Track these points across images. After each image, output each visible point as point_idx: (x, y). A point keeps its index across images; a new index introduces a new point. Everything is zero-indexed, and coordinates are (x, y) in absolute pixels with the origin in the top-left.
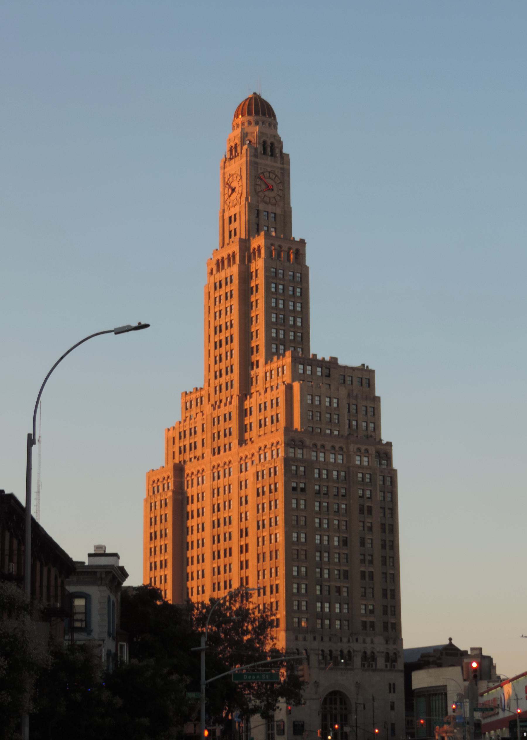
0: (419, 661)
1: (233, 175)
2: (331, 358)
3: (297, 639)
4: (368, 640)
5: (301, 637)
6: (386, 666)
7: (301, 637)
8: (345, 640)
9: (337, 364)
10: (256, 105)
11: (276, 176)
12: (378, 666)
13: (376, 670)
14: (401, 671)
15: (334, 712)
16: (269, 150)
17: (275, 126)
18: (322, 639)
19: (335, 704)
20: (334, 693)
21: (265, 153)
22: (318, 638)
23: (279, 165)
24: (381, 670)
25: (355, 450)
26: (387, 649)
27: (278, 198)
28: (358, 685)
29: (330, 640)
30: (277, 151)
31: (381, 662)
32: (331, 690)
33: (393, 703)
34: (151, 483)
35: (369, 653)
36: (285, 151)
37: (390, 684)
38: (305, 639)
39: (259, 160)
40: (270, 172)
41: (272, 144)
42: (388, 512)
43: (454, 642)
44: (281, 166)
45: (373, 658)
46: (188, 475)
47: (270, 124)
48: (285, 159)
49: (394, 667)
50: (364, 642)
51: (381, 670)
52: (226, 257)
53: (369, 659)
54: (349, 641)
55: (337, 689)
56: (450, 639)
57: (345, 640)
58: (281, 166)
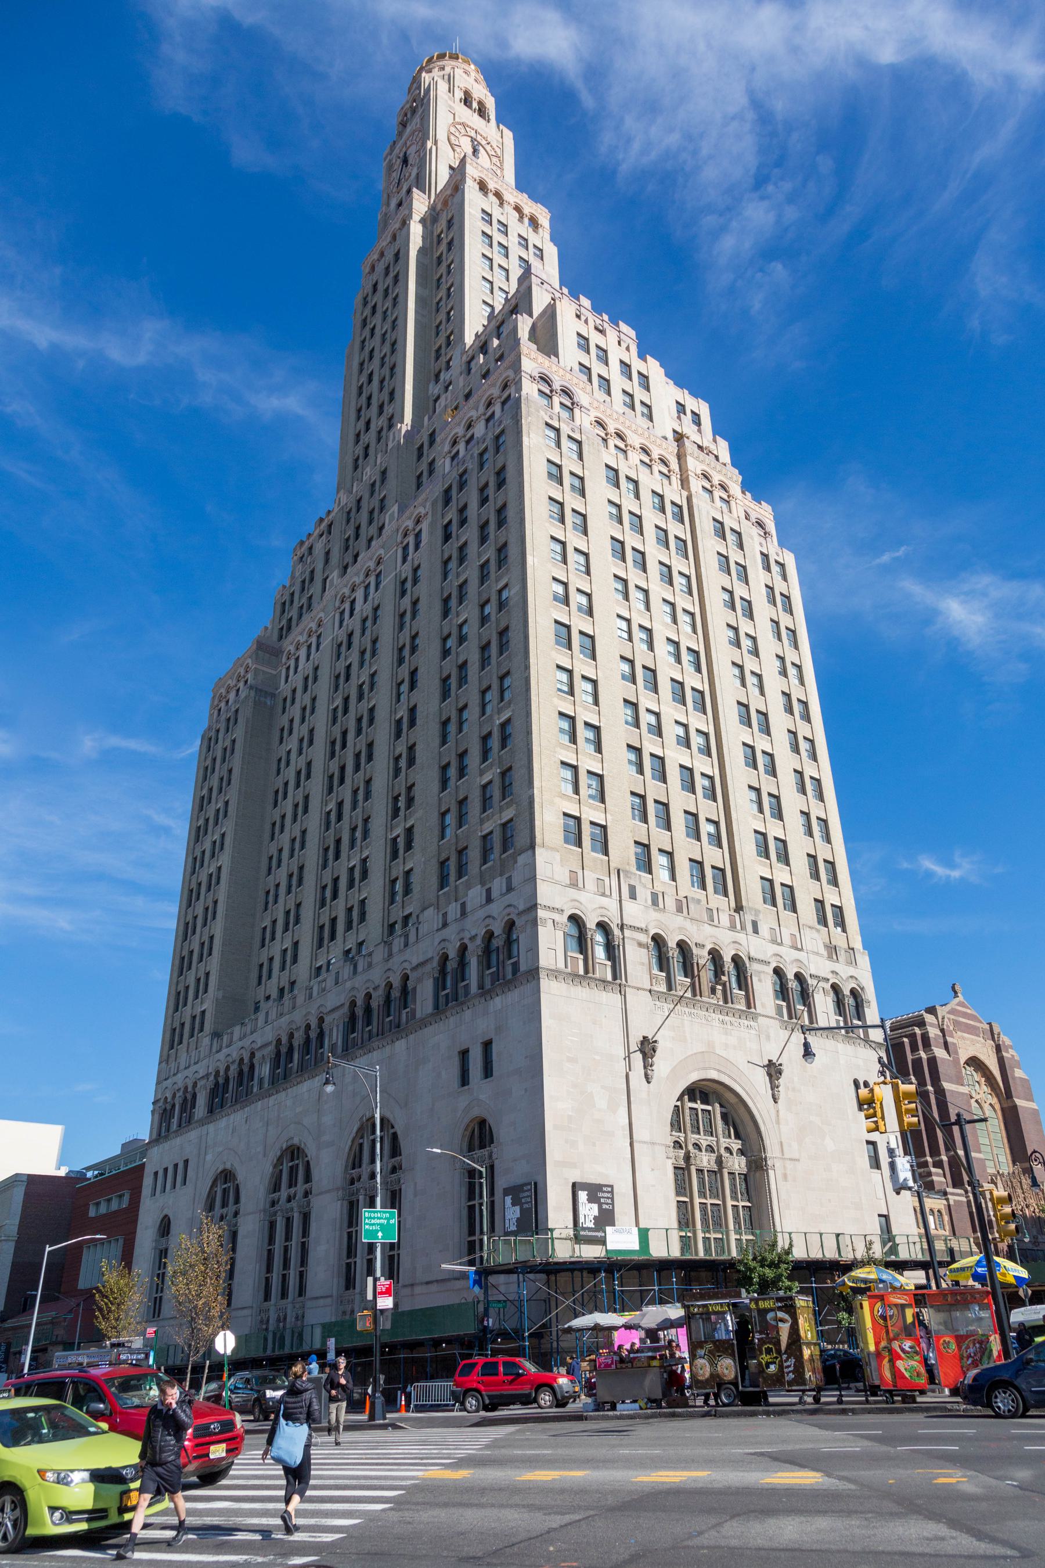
8: (725, 919)
28: (773, 1070)
29: (679, 910)
32: (694, 1077)
54: (733, 927)
55: (713, 1075)
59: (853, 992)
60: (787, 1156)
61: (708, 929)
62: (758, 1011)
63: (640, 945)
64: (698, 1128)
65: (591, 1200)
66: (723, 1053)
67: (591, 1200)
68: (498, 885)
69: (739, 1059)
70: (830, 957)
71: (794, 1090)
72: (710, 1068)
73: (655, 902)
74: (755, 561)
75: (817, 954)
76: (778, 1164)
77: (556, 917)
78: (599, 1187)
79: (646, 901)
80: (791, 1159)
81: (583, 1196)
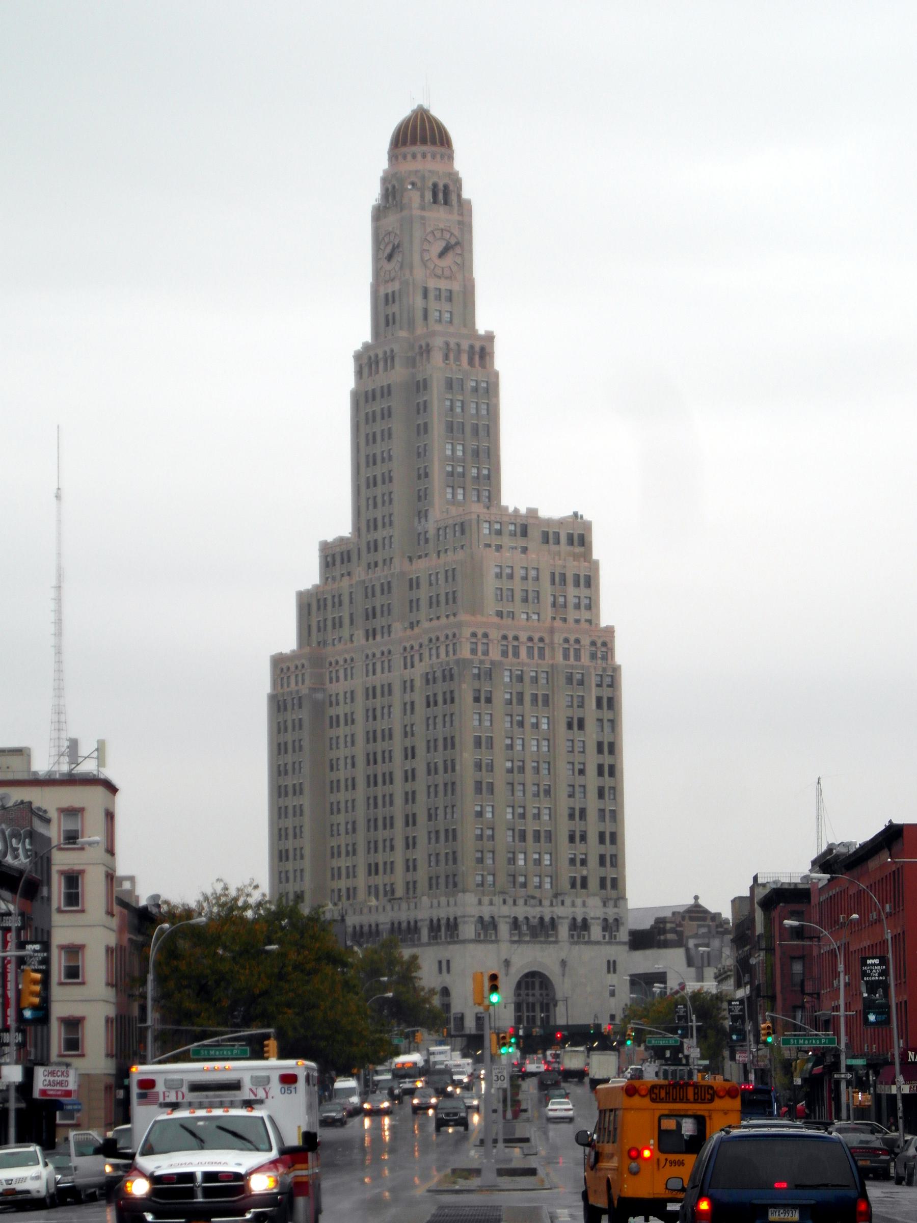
0: (652, 927)
1: (389, 233)
2: (528, 509)
3: (480, 903)
4: (579, 902)
5: (486, 900)
6: (604, 937)
7: (486, 900)
8: (546, 902)
9: (537, 518)
10: (423, 129)
11: (452, 234)
12: (593, 938)
13: (589, 942)
14: (624, 943)
16: (441, 196)
17: (451, 157)
18: (515, 903)
19: (533, 988)
20: (532, 975)
21: (435, 201)
22: (510, 901)
23: (456, 217)
24: (597, 943)
25: (561, 641)
26: (606, 913)
27: (454, 268)
28: (563, 963)
29: (526, 904)
30: (454, 197)
31: (596, 932)
32: (526, 971)
34: (279, 672)
35: (579, 920)
36: (465, 195)
37: (609, 962)
38: (491, 903)
39: (426, 214)
40: (442, 230)
41: (446, 187)
42: (606, 725)
43: (701, 902)
44: (460, 218)
45: (585, 925)
46: (331, 664)
47: (442, 157)
48: (464, 209)
49: (615, 938)
50: (573, 905)
51: (597, 943)
52: (381, 356)
53: (580, 927)
54: (552, 905)
56: (696, 898)
57: (546, 902)
58: (460, 218)
59: (616, 920)
61: (539, 909)
68: (452, 901)
70: (605, 905)
73: (515, 903)
77: (472, 919)
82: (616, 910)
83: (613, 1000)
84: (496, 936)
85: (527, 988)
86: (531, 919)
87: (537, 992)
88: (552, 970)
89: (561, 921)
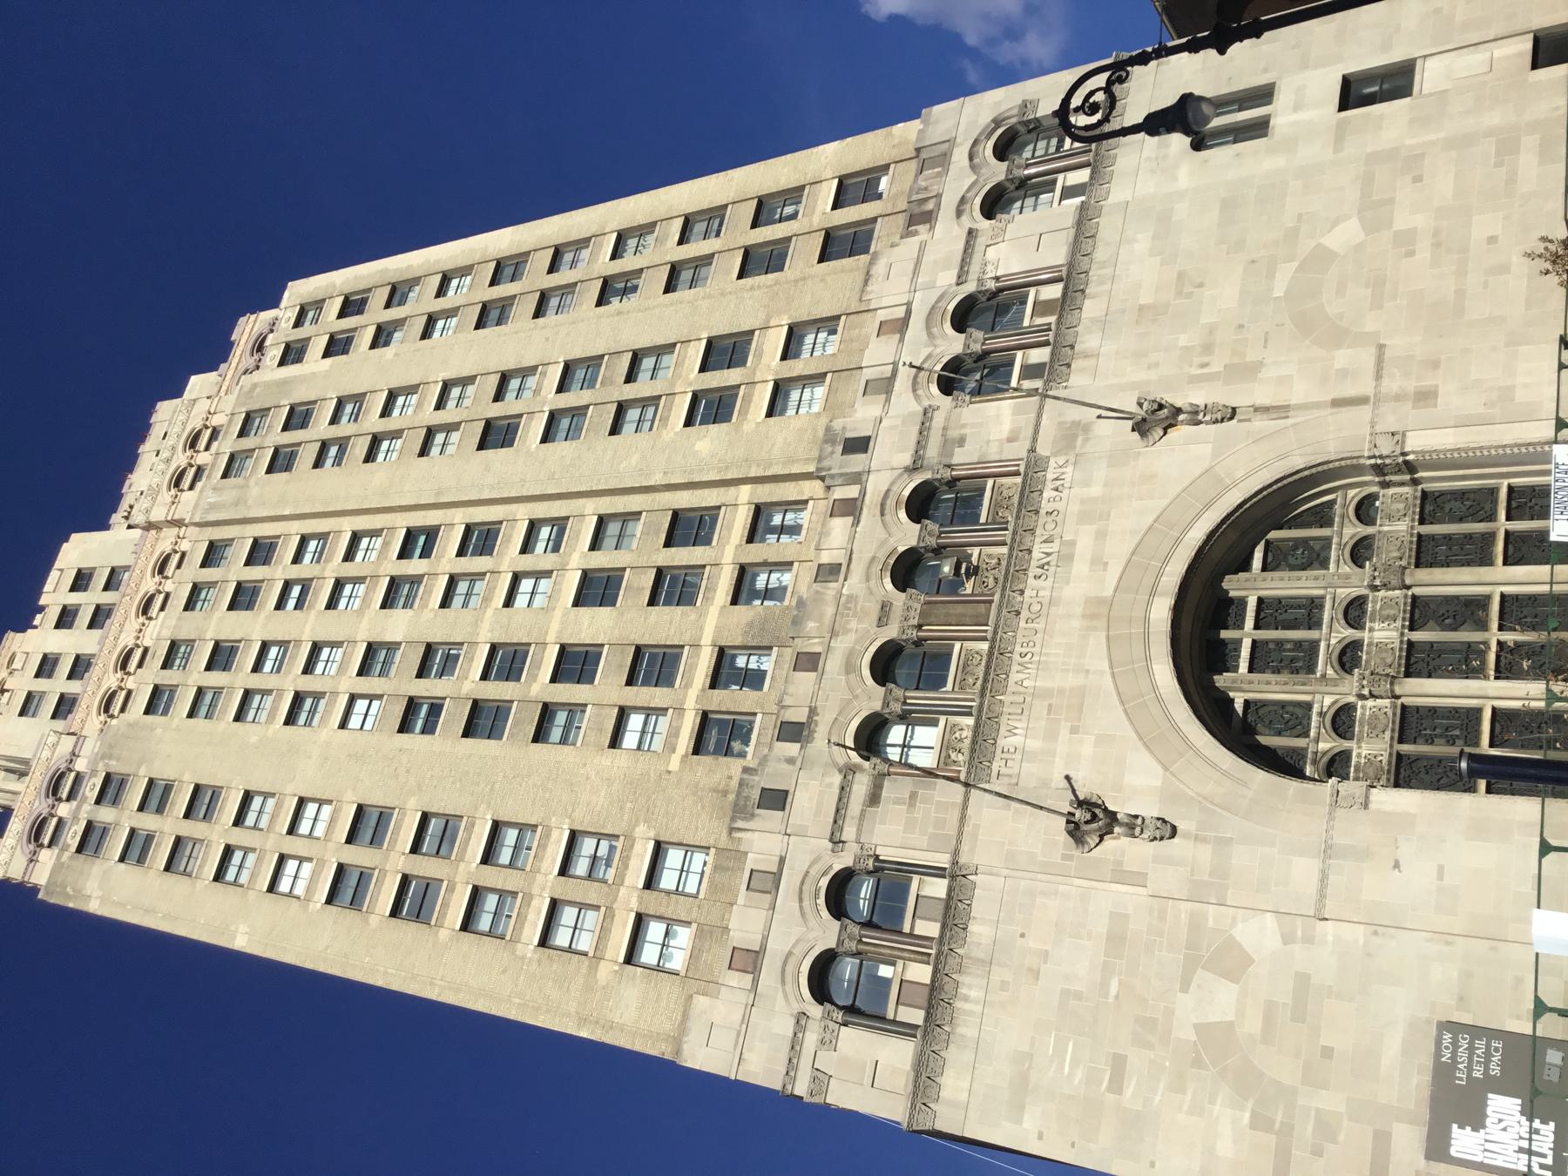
3: (749, 960)
4: (878, 354)
5: (745, 924)
6: (1068, 192)
13: (1072, 280)
15: (1383, 634)
19: (1309, 613)
20: (1201, 632)
28: (1155, 419)
33: (1353, 93)
38: (767, 882)
50: (884, 386)
54: (850, 508)
55: (1162, 611)
60: (1365, 387)
62: (1020, 450)
63: (874, 798)
64: (1298, 644)
65: (1478, 1123)
66: (1114, 571)
67: (1478, 1123)
69: (1130, 522)
71: (1207, 348)
72: (1146, 620)
74: (284, 382)
75: (918, 263)
76: (1389, 422)
77: (811, 1038)
78: (1442, 1073)
79: (791, 761)
80: (1378, 376)
81: (1464, 1142)
82: (960, 157)
83: (1429, 77)
84: (938, 872)
85: (1301, 660)
86: (891, 632)
87: (1337, 582)
88: (1207, 476)
89: (932, 452)
